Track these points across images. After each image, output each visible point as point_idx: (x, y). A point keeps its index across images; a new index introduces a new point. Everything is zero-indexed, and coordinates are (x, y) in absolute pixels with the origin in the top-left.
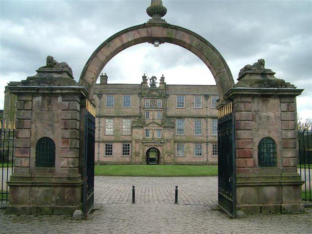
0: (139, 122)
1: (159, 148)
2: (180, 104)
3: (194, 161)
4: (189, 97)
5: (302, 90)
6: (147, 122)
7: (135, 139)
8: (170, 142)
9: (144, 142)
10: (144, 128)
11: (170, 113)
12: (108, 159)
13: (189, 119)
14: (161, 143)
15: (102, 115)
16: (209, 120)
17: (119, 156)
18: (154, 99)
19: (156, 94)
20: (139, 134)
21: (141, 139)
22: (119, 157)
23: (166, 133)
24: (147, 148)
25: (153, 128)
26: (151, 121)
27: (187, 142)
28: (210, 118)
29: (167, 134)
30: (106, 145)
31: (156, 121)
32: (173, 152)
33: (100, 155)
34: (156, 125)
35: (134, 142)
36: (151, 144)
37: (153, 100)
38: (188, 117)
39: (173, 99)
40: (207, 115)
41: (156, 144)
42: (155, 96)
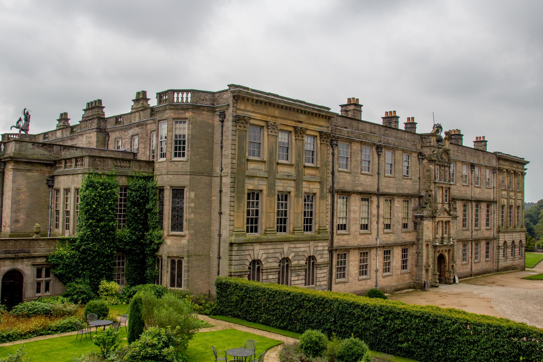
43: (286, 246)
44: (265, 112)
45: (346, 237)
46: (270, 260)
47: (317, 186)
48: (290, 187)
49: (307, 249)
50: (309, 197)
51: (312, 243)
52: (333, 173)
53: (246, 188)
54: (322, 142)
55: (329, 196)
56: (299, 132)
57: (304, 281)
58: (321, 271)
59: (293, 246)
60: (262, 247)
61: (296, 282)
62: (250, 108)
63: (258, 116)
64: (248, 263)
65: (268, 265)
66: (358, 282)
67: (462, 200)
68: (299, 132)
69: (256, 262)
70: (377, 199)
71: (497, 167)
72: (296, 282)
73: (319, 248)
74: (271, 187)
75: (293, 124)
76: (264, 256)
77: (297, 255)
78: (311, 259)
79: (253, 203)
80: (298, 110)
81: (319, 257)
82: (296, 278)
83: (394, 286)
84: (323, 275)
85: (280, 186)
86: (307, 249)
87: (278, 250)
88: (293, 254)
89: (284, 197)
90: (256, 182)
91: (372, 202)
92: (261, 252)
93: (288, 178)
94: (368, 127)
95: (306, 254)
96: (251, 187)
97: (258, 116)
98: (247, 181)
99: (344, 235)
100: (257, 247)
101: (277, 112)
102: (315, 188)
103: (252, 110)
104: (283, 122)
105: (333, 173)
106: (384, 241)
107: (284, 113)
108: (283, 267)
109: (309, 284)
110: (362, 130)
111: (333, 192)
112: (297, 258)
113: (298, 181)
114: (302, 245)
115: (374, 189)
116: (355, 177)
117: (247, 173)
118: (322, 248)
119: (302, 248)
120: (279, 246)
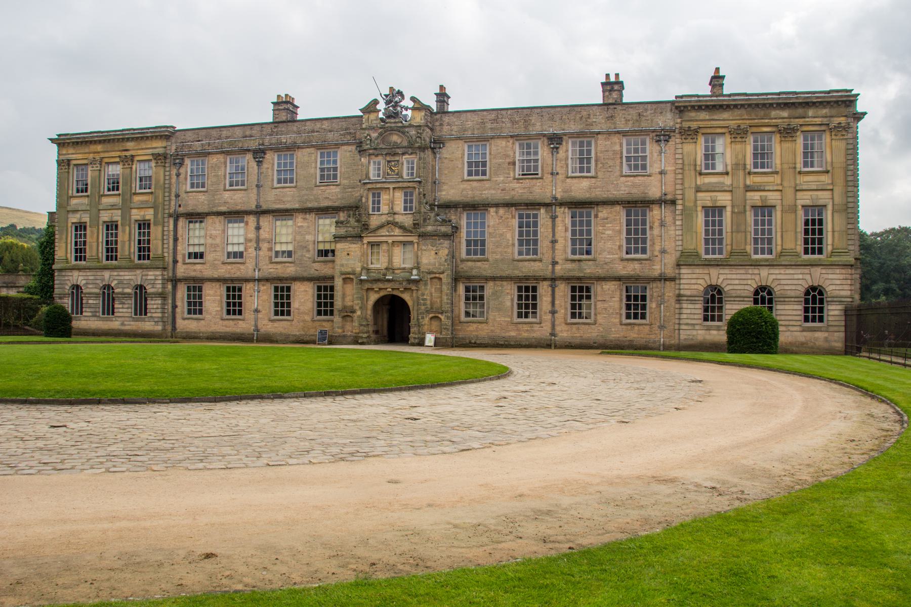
0: (354, 218)
1: (406, 297)
2: (478, 168)
3: (513, 334)
4: (503, 143)
5: (865, 114)
6: (374, 221)
7: (344, 269)
8: (440, 279)
9: (369, 282)
10: (365, 241)
11: (450, 192)
12: (281, 326)
13: (502, 211)
14: (410, 281)
15: (265, 207)
16: (559, 211)
17: (308, 318)
18: (395, 154)
19: (399, 141)
20: (351, 257)
22: (304, 321)
24: (374, 297)
25: (390, 240)
26: (384, 219)
27: (494, 279)
28: (561, 204)
29: (432, 257)
30: (276, 289)
31: (399, 219)
32: (446, 307)
33: (260, 316)
34: (397, 231)
36: (381, 285)
37: (393, 159)
38: (497, 205)
39: (456, 154)
40: (556, 199)
42: (397, 146)
43: (107, 274)
44: (87, 150)
45: (198, 267)
46: (90, 286)
47: (151, 211)
48: (117, 216)
49: (133, 277)
50: (144, 225)
51: (138, 272)
52: (177, 196)
54: (833, 137)
56: (128, 160)
58: (153, 302)
59: (115, 273)
60: (81, 273)
61: (121, 310)
62: (71, 151)
63: (80, 156)
64: (68, 288)
65: (88, 291)
66: (221, 322)
67: (547, 205)
68: (128, 160)
69: (77, 287)
70: (255, 219)
71: (678, 126)
72: (121, 310)
73: (149, 277)
74: (95, 219)
75: (118, 154)
76: (84, 282)
77: (120, 282)
78: (141, 287)
79: (81, 235)
80: (123, 139)
81: (150, 286)
82: (121, 306)
83: (295, 335)
84: (155, 306)
85: (105, 216)
86: (133, 277)
87: (98, 277)
88: (116, 282)
89: (111, 226)
90: (78, 216)
91: (247, 224)
92: (80, 278)
93: (113, 207)
94: (239, 132)
95: (132, 283)
96: (75, 220)
97: (80, 156)
98: (70, 215)
99: (195, 264)
100: (76, 273)
101: (99, 148)
102: (149, 214)
103: (74, 152)
104: (106, 155)
106: (270, 273)
107: (108, 146)
108: (109, 294)
109: (141, 314)
110: (227, 137)
112: (120, 286)
113: (126, 208)
114: (127, 273)
115: (253, 207)
116: (213, 196)
117: (69, 208)
118: (153, 277)
119: (127, 275)
120: (99, 274)
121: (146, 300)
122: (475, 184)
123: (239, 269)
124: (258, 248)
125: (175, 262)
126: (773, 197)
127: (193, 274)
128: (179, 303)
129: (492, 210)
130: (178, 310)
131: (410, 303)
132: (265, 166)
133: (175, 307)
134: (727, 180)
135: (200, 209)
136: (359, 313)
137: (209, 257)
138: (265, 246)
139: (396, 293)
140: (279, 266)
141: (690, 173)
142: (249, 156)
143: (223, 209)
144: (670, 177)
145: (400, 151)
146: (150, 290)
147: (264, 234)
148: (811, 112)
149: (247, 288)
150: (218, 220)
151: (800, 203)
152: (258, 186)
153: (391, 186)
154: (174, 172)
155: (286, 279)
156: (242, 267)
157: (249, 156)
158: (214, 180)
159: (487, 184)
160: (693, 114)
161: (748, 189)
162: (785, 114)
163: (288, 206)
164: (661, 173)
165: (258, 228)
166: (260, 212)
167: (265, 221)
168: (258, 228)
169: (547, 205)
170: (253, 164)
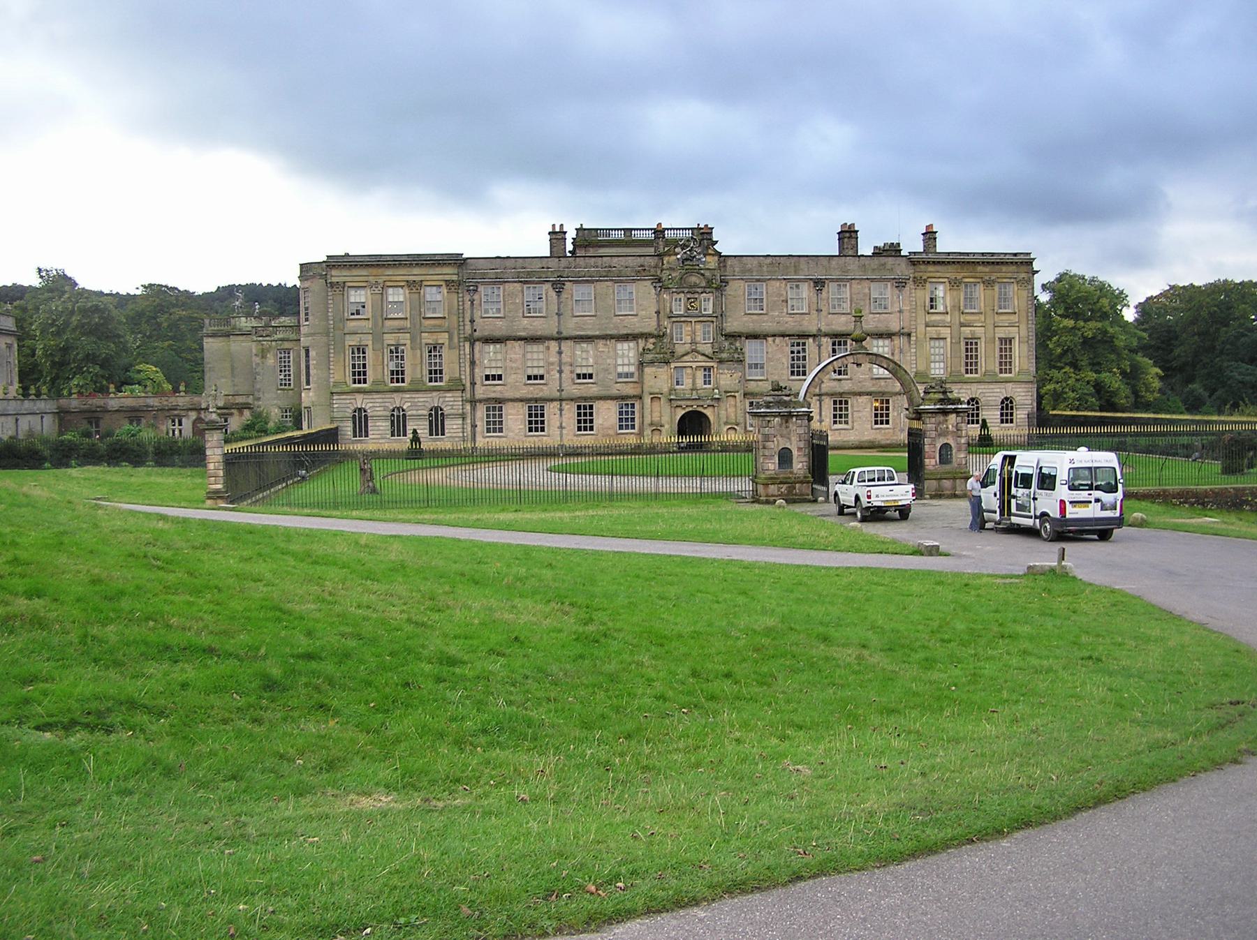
0: (657, 348)
6: (680, 350)
10: (673, 365)
11: (732, 325)
12: (586, 440)
13: (778, 340)
15: (565, 334)
16: (824, 340)
20: (658, 379)
21: (665, 390)
23: (723, 376)
24: (680, 413)
28: (826, 335)
29: (726, 378)
30: (579, 408)
31: (700, 348)
32: (741, 420)
33: (565, 432)
34: (701, 358)
35: (647, 400)
36: (689, 403)
38: (774, 336)
39: (737, 289)
40: (819, 330)
41: (701, 403)
42: (696, 286)
47: (446, 335)
51: (435, 394)
52: (472, 321)
53: (347, 343)
55: (467, 345)
57: (427, 431)
91: (548, 348)
100: (359, 397)
105: (472, 321)
111: (472, 341)
119: (421, 398)
121: (443, 422)
122: (755, 317)
123: (542, 390)
124: (560, 372)
125: (473, 384)
126: (979, 331)
127: (493, 395)
128: (478, 423)
129: (770, 339)
130: (478, 429)
131: (711, 418)
132: (564, 295)
133: (474, 426)
134: (948, 318)
135: (497, 334)
136: (667, 426)
137: (510, 379)
138: (566, 369)
139: (700, 409)
140: (582, 387)
141: (921, 313)
142: (548, 286)
143: (523, 334)
144: (906, 314)
145: (699, 290)
146: (447, 410)
147: (565, 358)
148: (1004, 268)
149: (597, 405)
150: (517, 344)
151: (998, 335)
152: (558, 314)
153: (693, 320)
154: (467, 298)
155: (591, 398)
156: (545, 388)
157: (548, 286)
158: (512, 307)
159: (766, 318)
160: (923, 267)
161: (962, 325)
162: (987, 269)
163: (590, 333)
164: (900, 312)
165: (560, 353)
166: (559, 338)
167: (566, 346)
168: (560, 353)
169: (814, 336)
170: (553, 294)
